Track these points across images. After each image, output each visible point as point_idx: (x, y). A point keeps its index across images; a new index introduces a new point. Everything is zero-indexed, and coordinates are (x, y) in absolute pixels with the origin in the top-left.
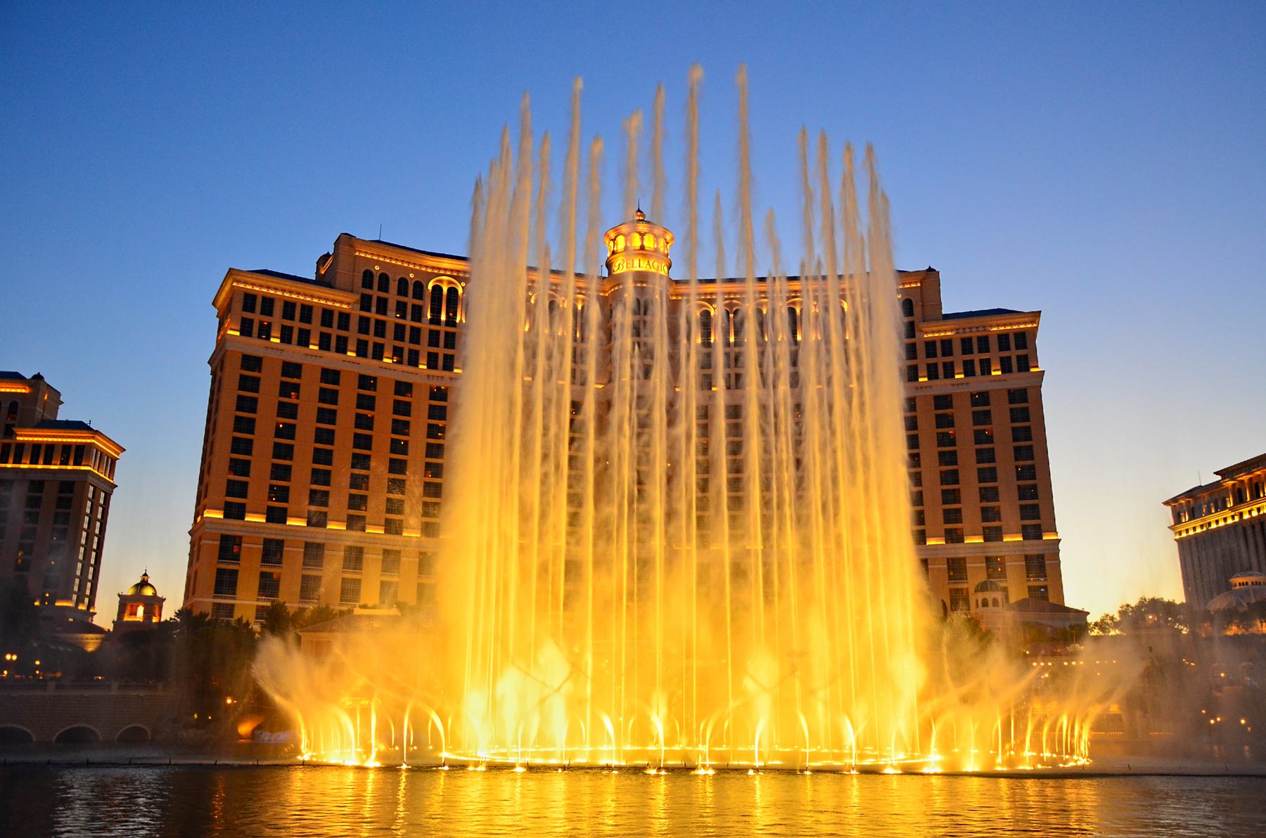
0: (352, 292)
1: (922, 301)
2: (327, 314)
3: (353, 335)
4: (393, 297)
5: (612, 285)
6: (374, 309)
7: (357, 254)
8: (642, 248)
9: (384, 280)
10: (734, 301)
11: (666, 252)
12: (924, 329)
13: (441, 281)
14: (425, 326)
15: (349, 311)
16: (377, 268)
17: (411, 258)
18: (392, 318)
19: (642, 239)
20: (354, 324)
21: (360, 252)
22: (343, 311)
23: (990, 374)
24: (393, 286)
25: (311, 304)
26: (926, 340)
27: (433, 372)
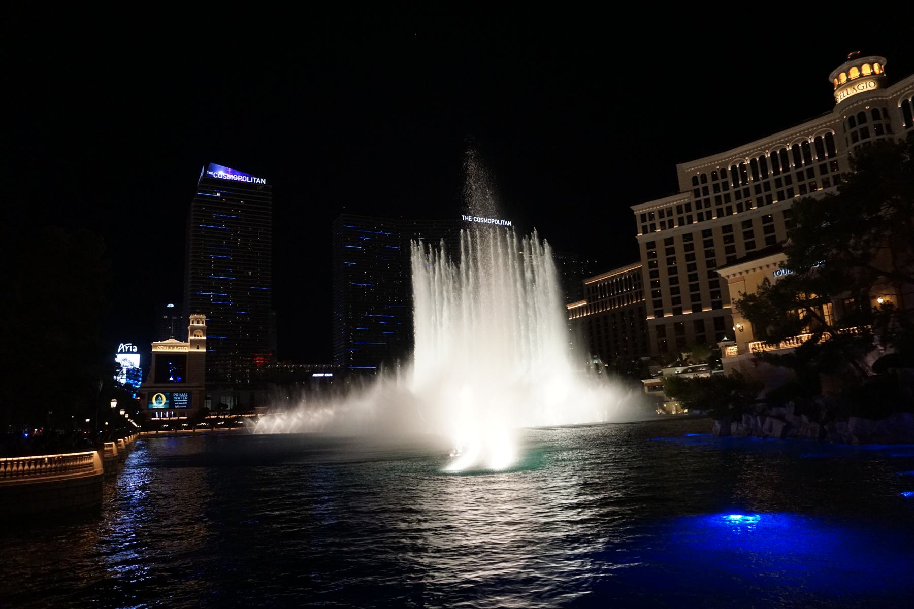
2: (679, 209)
3: (694, 212)
4: (710, 184)
6: (702, 194)
8: (849, 80)
9: (704, 178)
11: (872, 71)
15: (689, 202)
16: (698, 173)
18: (712, 195)
20: (693, 206)
21: (687, 169)
22: (687, 202)
24: (709, 178)
25: (670, 206)
27: (741, 214)
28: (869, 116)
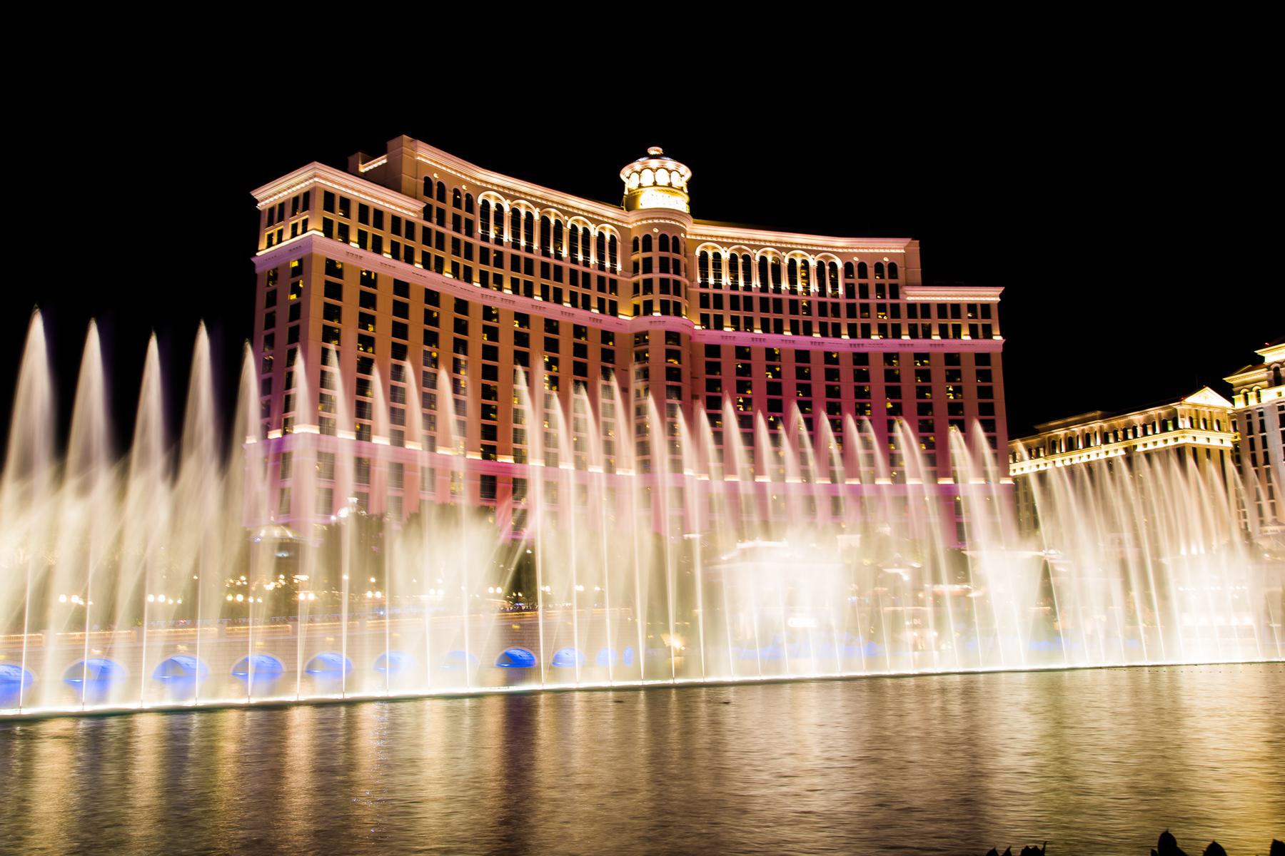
0: (415, 198)
1: (905, 267)
2: (396, 220)
5: (639, 218)
7: (419, 158)
8: (670, 185)
10: (743, 247)
12: (907, 292)
13: (488, 196)
14: (477, 242)
17: (464, 168)
18: (448, 231)
19: (670, 176)
20: (419, 234)
23: (960, 337)
24: (449, 195)
26: (908, 302)
28: (682, 245)
